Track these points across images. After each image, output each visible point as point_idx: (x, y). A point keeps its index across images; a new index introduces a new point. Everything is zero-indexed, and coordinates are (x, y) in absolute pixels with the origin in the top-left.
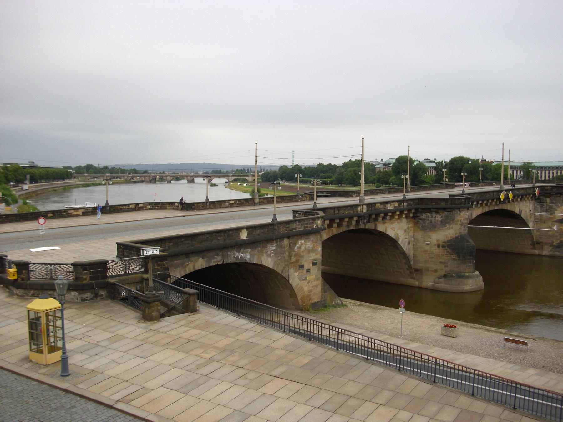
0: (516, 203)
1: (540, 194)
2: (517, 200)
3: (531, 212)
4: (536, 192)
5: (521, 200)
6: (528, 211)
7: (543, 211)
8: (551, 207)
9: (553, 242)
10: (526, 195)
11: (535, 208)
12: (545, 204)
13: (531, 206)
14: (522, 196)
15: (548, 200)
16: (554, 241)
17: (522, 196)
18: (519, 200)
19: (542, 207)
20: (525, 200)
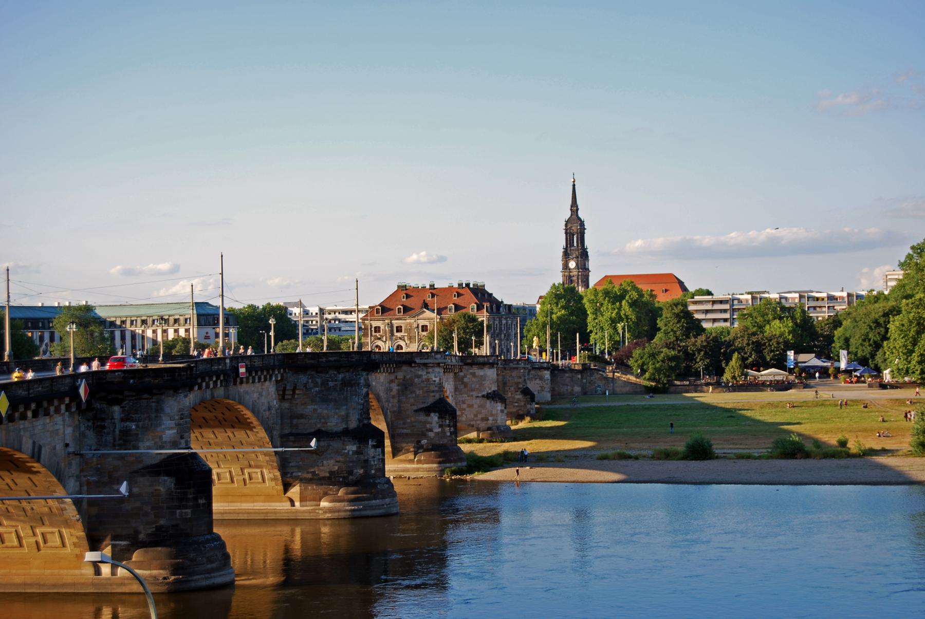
0: (22, 424)
1: (91, 394)
2: (24, 417)
3: (71, 449)
4: (82, 391)
5: (35, 415)
6: (59, 447)
7: (105, 445)
8: (125, 433)
9: (137, 533)
10: (50, 402)
11: (80, 438)
12: (107, 423)
13: (69, 430)
14: (39, 405)
15: (116, 409)
16: (141, 528)
17: (39, 405)
18: (29, 414)
19: (99, 430)
20: (47, 414)
